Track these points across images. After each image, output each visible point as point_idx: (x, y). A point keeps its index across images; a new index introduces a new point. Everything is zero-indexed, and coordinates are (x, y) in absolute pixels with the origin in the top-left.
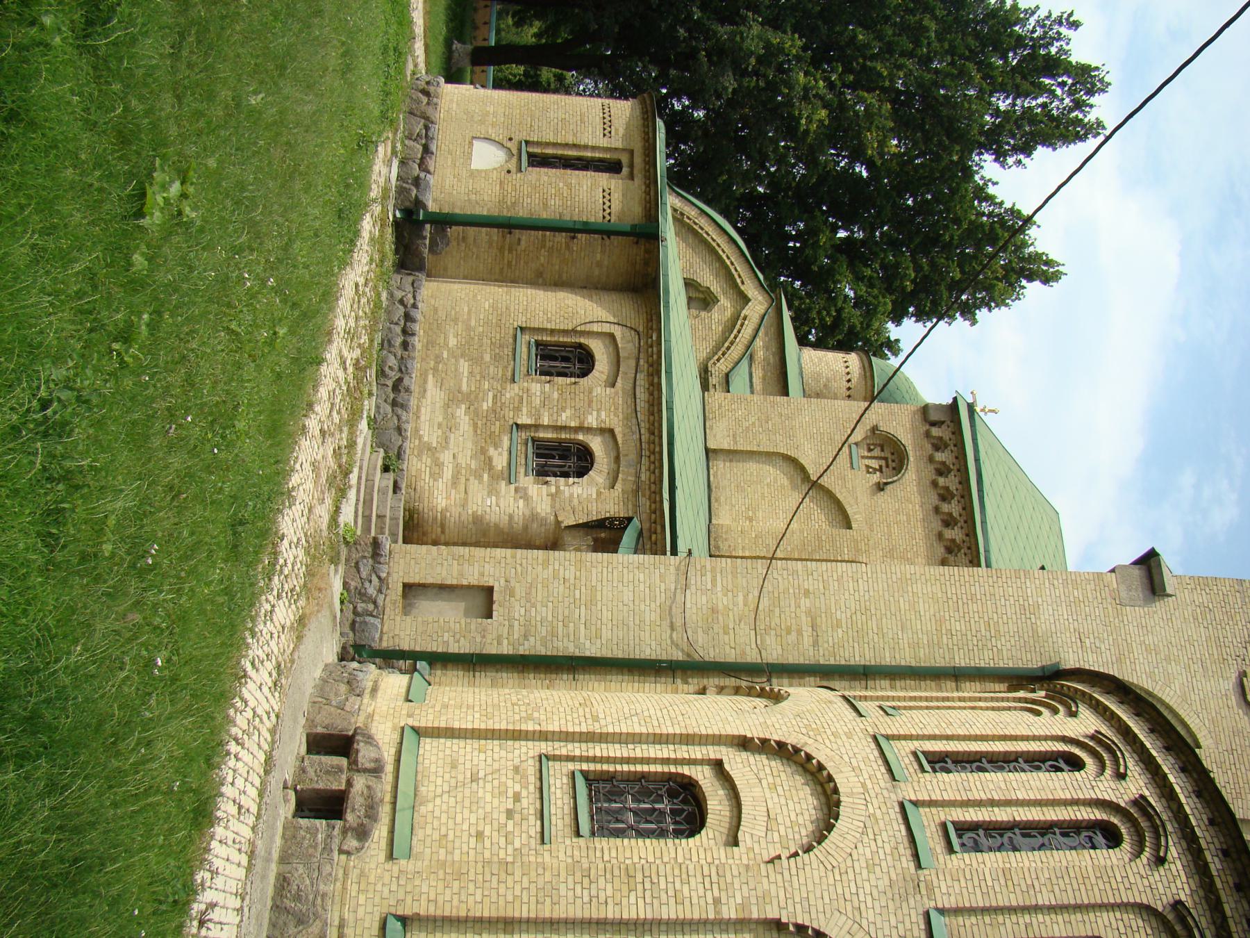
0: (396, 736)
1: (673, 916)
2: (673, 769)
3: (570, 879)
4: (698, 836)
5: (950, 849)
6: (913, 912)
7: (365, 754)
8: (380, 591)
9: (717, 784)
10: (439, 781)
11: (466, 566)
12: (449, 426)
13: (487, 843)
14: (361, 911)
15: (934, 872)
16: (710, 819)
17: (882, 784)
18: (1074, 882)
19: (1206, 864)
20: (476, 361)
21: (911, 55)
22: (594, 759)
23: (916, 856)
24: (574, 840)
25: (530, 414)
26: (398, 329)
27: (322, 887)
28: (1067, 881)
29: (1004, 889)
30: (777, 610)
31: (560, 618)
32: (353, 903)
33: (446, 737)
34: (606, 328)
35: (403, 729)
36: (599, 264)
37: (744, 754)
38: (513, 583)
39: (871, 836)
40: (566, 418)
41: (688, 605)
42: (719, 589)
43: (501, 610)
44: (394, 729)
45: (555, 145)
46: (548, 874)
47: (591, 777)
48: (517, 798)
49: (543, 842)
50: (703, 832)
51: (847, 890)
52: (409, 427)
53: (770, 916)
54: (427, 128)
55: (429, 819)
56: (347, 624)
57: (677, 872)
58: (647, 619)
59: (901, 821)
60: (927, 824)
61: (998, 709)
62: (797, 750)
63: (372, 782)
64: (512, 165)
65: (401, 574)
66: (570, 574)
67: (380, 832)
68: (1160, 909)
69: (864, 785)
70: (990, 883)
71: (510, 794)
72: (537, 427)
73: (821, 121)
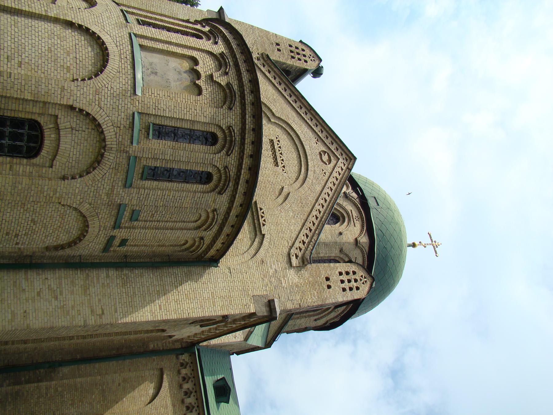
19: (232, 46)
53: (68, 19)
61: (161, 15)
68: (215, 53)
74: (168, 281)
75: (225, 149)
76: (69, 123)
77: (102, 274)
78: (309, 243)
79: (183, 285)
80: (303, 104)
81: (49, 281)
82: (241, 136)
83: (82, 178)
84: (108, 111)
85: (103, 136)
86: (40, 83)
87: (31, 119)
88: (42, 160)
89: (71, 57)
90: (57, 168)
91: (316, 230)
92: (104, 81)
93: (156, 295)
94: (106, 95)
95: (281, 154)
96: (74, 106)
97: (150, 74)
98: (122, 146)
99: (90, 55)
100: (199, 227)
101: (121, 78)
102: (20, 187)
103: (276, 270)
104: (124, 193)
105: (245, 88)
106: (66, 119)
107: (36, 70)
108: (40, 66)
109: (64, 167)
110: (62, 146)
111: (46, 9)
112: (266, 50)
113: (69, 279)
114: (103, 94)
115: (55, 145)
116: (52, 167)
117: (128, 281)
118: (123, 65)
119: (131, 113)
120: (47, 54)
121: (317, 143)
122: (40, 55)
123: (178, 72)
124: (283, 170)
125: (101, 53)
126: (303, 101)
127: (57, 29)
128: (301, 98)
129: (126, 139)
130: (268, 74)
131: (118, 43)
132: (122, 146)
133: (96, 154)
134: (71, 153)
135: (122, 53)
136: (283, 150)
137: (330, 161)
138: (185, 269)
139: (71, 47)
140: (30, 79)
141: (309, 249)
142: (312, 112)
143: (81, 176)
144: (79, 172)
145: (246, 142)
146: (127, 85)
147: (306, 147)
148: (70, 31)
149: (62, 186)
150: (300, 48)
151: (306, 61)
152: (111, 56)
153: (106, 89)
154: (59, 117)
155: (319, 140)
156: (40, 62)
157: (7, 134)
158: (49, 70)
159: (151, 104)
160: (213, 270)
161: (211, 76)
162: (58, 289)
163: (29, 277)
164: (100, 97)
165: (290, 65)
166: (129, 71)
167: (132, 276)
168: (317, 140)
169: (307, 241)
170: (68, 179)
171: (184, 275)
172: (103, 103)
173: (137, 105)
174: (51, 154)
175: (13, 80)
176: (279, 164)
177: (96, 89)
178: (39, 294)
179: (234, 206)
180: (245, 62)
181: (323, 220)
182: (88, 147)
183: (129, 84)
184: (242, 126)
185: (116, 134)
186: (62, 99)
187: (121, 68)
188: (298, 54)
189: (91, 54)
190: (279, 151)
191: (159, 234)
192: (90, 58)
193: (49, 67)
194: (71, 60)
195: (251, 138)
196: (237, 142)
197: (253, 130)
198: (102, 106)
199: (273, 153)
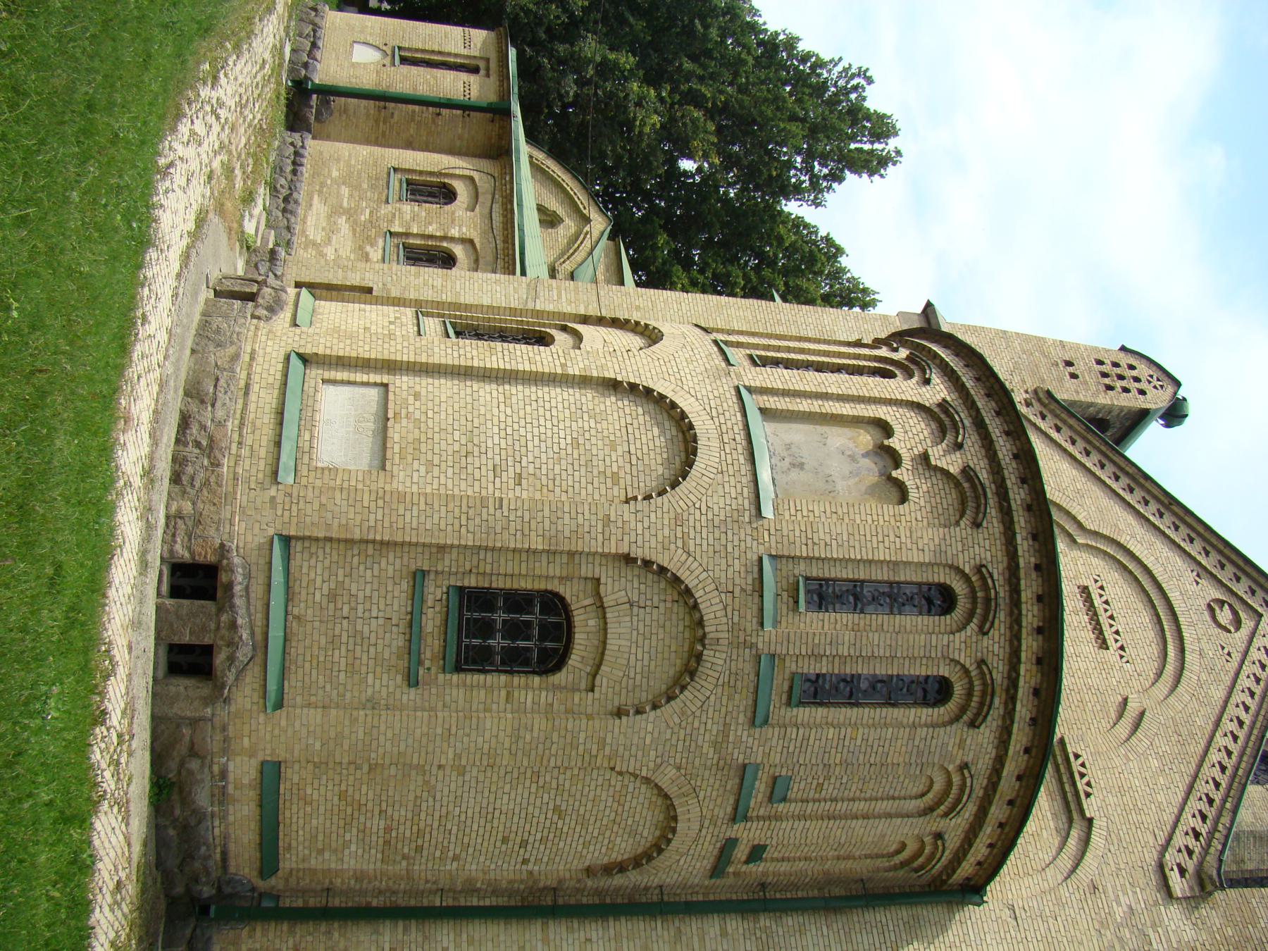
11: (349, 273)
12: (332, 230)
14: (269, 350)
19: (963, 385)
20: (356, 187)
21: (731, 84)
25: (401, 225)
26: (289, 161)
34: (467, 173)
36: (460, 138)
38: (389, 286)
40: (431, 230)
42: (564, 299)
45: (423, 51)
52: (298, 228)
53: (607, 375)
54: (314, 31)
61: (800, 339)
64: (388, 61)
72: (407, 235)
73: (654, 125)
74: (866, 942)
75: (975, 620)
76: (623, 593)
77: (712, 930)
78: (1211, 834)
80: (1149, 492)
82: (1010, 586)
84: (705, 560)
85: (697, 615)
86: (560, 514)
87: (546, 591)
88: (571, 677)
89: (620, 452)
91: (1224, 801)
92: (691, 496)
94: (698, 524)
95: (1111, 617)
96: (632, 555)
98: (742, 634)
99: (657, 444)
100: (931, 809)
101: (726, 485)
102: (528, 737)
103: (1130, 908)
104: (750, 740)
105: (1006, 472)
106: (617, 583)
107: (551, 487)
108: (558, 477)
109: (617, 688)
111: (563, 361)
112: (1043, 380)
113: (637, 941)
114: (692, 524)
115: (596, 642)
116: (592, 690)
119: (755, 557)
120: (569, 452)
121: (1197, 583)
124: (1122, 657)
125: (680, 435)
126: (1147, 485)
127: (588, 398)
128: (1142, 480)
129: (749, 617)
130: (1055, 435)
132: (742, 634)
133: (686, 655)
134: (633, 658)
136: (1116, 608)
137: (1238, 623)
138: (904, 913)
139: (618, 434)
140: (540, 507)
141: (1212, 850)
142: (1175, 508)
144: (650, 697)
145: (1023, 599)
146: (740, 498)
147: (1174, 596)
148: (613, 399)
149: (616, 730)
150: (1123, 363)
151: (1142, 392)
153: (698, 512)
154: (603, 580)
155: (1203, 573)
156: (557, 471)
157: (499, 626)
158: (577, 485)
159: (797, 534)
160: (972, 912)
161: (925, 457)
163: (552, 936)
164: (686, 530)
165: (1104, 406)
166: (743, 467)
167: (781, 933)
168: (1198, 575)
169: (1204, 830)
172: (692, 542)
173: (767, 538)
174: (591, 662)
175: (506, 514)
176: (1110, 642)
177: (677, 514)
179: (1011, 752)
180: (998, 414)
181: (1240, 772)
183: (746, 495)
184: (1009, 564)
185: (725, 608)
187: (724, 463)
188: (1121, 377)
189: (660, 442)
190: (1106, 610)
191: (837, 830)
192: (658, 450)
193: (577, 479)
194: (620, 459)
195: (1035, 589)
196: (1001, 601)
197: (1037, 567)
198: (692, 549)
199: (1091, 619)
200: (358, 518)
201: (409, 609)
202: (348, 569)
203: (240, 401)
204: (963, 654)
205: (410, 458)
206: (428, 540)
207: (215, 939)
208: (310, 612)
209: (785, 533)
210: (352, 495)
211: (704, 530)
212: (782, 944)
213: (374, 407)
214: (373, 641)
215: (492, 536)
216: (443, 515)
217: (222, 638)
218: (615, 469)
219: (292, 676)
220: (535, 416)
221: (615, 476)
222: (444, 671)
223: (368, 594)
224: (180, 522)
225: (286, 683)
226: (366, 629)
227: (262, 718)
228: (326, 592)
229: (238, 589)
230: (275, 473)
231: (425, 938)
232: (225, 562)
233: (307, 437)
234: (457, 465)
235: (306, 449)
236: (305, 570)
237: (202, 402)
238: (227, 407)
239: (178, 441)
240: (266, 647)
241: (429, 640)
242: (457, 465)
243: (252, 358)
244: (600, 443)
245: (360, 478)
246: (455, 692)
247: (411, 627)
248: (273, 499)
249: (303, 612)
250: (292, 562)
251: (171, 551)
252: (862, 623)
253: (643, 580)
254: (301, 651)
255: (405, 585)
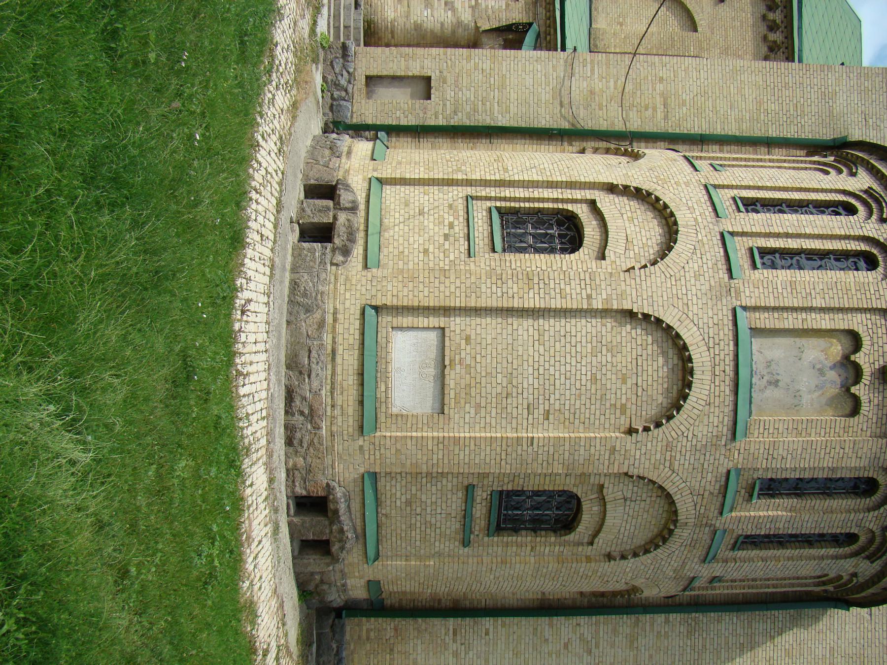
0: (366, 185)
1: (559, 306)
2: (560, 206)
3: (488, 280)
4: (577, 253)
5: (754, 266)
6: (724, 308)
7: (345, 198)
8: (349, 82)
9: (591, 216)
10: (397, 215)
13: (431, 257)
14: (347, 303)
15: (741, 281)
16: (586, 241)
17: (709, 219)
18: (840, 292)
22: (505, 199)
23: (729, 270)
24: (491, 254)
27: (320, 288)
28: (835, 291)
29: (790, 295)
30: (639, 92)
31: (480, 99)
32: (342, 298)
33: (401, 184)
35: (370, 179)
37: (611, 196)
39: (699, 256)
41: (573, 88)
42: (596, 76)
43: (437, 93)
44: (364, 179)
46: (473, 279)
47: (503, 211)
48: (451, 226)
49: (469, 256)
50: (581, 250)
51: (679, 292)
53: (625, 307)
55: (391, 241)
56: (328, 107)
57: (562, 277)
58: (543, 99)
59: (720, 245)
60: (739, 248)
62: (649, 194)
63: (351, 216)
65: (364, 69)
66: (487, 66)
67: (358, 251)
69: (696, 220)
70: (780, 291)
71: (446, 223)
74: (761, 629)
79: (784, 635)
81: (582, 628)
83: (637, 559)
84: (685, 475)
85: (673, 509)
86: (577, 448)
88: (577, 537)
89: (629, 385)
90: (600, 544)
92: (682, 427)
93: (738, 650)
96: (630, 474)
97: (766, 387)
99: (660, 375)
101: (711, 415)
102: (545, 570)
108: (578, 411)
109: (610, 543)
110: (609, 521)
111: (589, 291)
114: (679, 449)
116: (591, 543)
117: (697, 629)
118: (717, 388)
119: (725, 471)
120: (588, 387)
122: (578, 392)
123: (819, 370)
129: (712, 510)
131: (711, 339)
133: (661, 526)
134: (622, 529)
135: (717, 363)
139: (629, 367)
140: (562, 443)
143: (635, 555)
144: (632, 547)
146: (721, 426)
148: (629, 327)
152: (697, 375)
154: (606, 486)
156: (577, 406)
158: (592, 416)
159: (761, 451)
162: (594, 640)
164: (673, 454)
166: (727, 398)
170: (615, 560)
171: (788, 619)
172: (677, 463)
173: (736, 456)
178: (566, 646)
182: (649, 520)
183: (725, 423)
185: (695, 505)
186: (611, 466)
189: (664, 371)
192: (660, 381)
193: (592, 412)
194: (629, 391)
198: (676, 468)
200: (425, 458)
201: (463, 508)
202: (419, 487)
203: (329, 367)
204: (872, 524)
205: (463, 401)
206: (477, 471)
207: (346, 623)
208: (393, 512)
209: (752, 451)
210: (420, 441)
211: (688, 454)
212: (704, 628)
213: (433, 353)
214: (438, 525)
215: (525, 465)
216: (488, 452)
217: (335, 537)
218: (624, 401)
219: (385, 544)
220: (563, 354)
221: (623, 409)
222: (488, 535)
223: (434, 500)
224: (296, 472)
225: (380, 547)
226: (433, 520)
227: (366, 566)
228: (404, 500)
229: (341, 512)
230: (361, 428)
231: (475, 622)
232: (331, 497)
233: (383, 389)
234: (499, 406)
235: (383, 400)
236: (388, 488)
237: (301, 373)
238: (322, 373)
239: (286, 412)
240: (365, 536)
241: (478, 521)
242: (499, 406)
243: (335, 320)
244: (614, 377)
245: (425, 422)
246: (495, 548)
247: (464, 517)
248: (361, 447)
249: (388, 512)
250: (379, 483)
251: (293, 492)
252: (798, 506)
253: (636, 484)
254: (389, 531)
255: (460, 494)
